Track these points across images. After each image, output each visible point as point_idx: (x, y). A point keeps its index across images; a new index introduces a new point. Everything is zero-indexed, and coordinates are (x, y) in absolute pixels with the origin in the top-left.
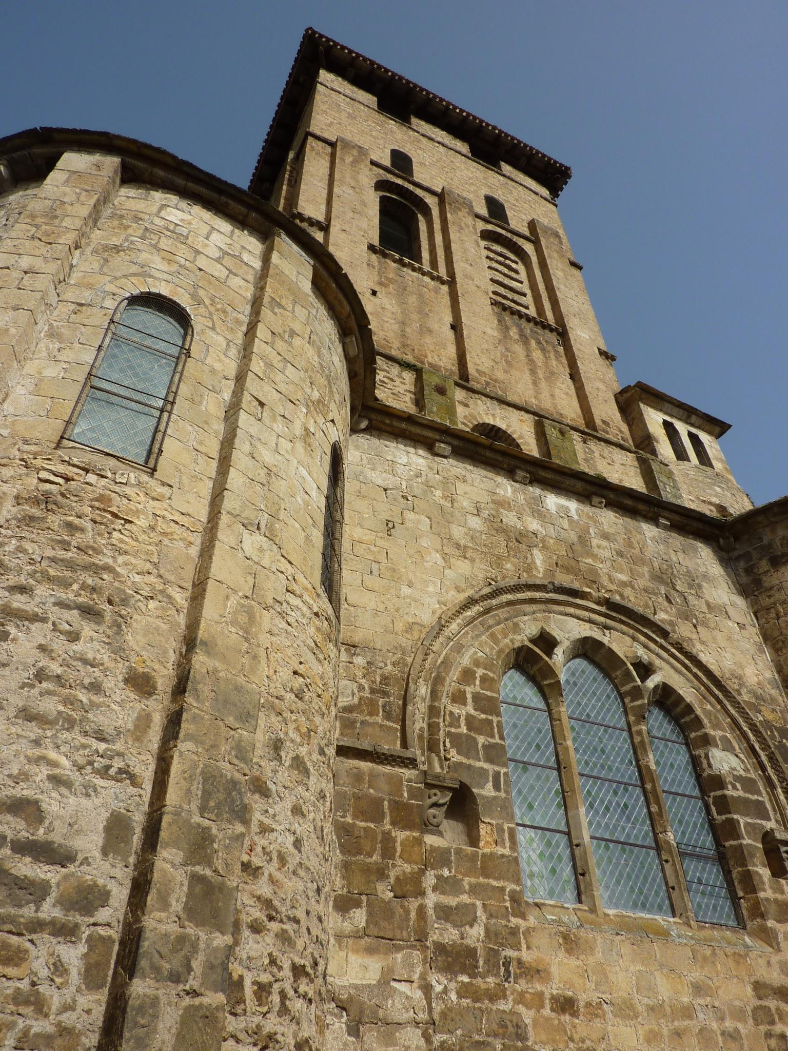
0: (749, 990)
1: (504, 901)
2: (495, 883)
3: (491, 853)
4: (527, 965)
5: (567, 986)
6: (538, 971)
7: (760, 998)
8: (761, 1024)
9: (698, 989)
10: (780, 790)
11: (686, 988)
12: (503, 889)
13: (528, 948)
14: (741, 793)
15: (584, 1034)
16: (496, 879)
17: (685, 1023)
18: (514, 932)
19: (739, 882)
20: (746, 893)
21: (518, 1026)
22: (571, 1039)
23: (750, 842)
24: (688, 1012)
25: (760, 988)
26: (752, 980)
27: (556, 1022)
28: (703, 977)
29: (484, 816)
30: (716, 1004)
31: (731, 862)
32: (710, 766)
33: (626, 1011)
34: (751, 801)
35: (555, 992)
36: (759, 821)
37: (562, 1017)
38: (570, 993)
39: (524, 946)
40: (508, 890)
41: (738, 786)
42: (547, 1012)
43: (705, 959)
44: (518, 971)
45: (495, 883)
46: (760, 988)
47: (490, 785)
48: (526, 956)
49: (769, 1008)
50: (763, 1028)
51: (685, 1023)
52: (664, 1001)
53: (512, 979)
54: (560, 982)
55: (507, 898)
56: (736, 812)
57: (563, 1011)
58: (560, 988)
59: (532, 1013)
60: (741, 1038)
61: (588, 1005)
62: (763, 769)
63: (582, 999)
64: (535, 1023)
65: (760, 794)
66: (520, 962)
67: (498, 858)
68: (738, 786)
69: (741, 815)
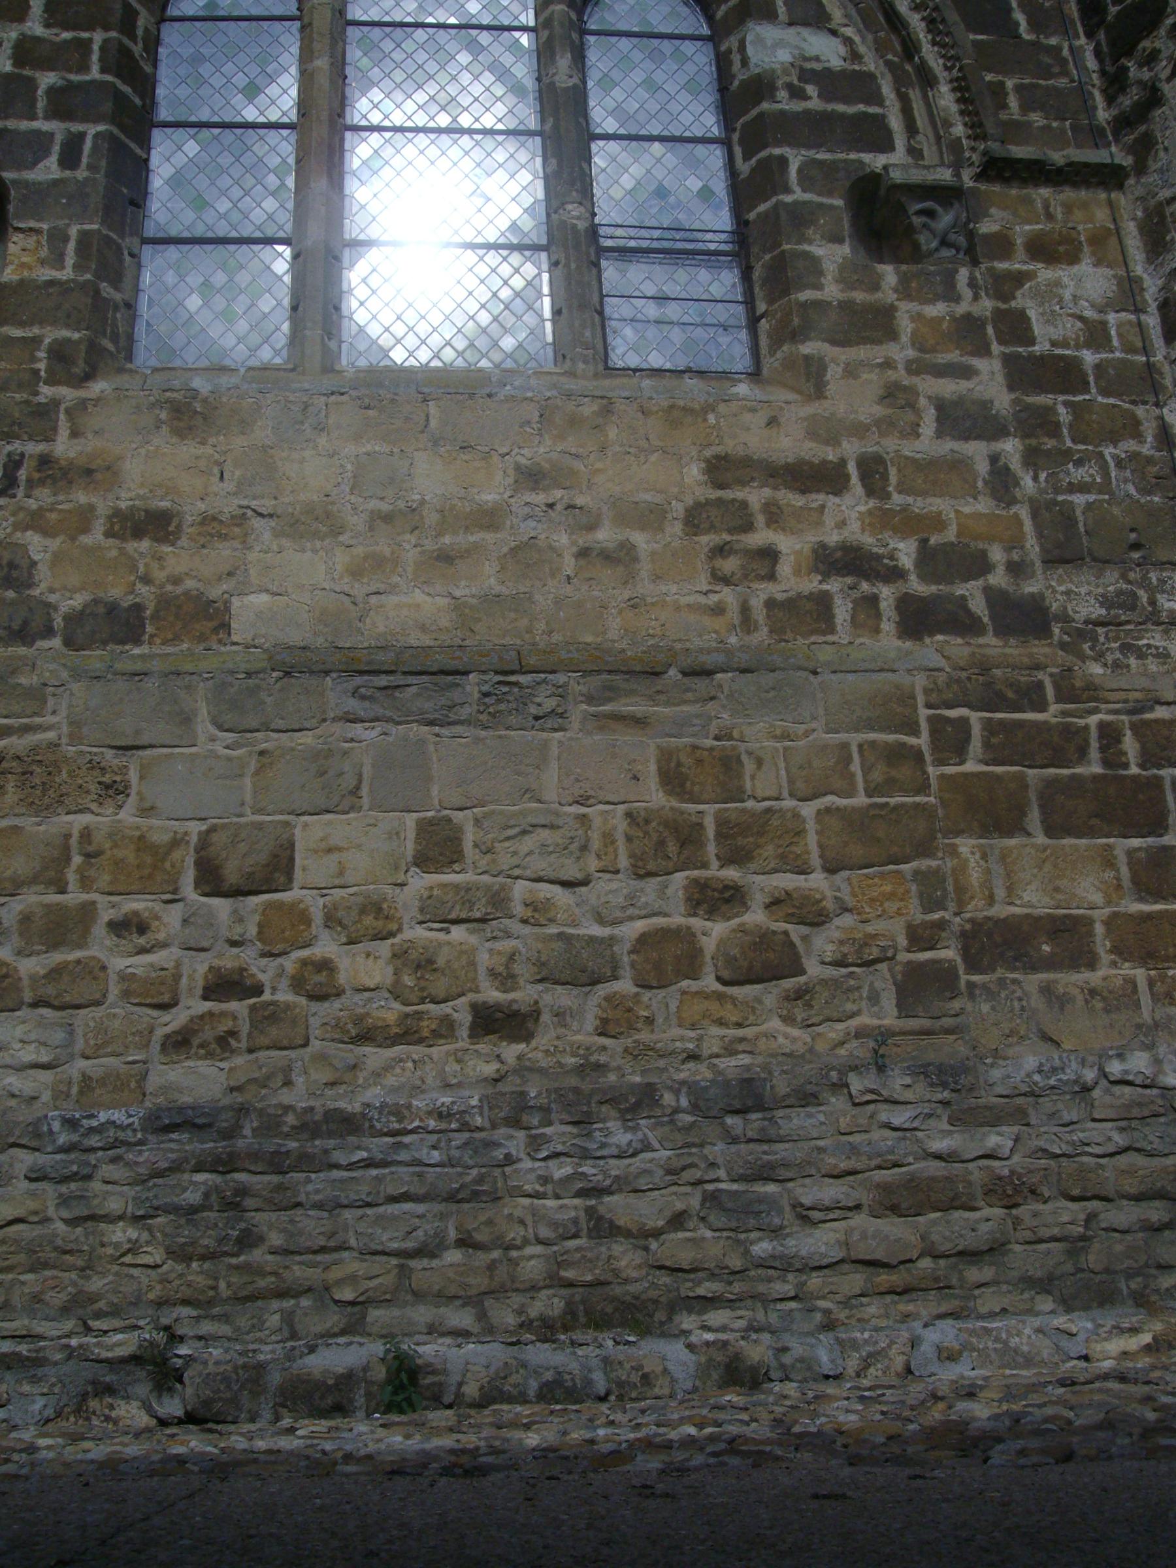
0: (694, 472)
1: (34, 359)
2: (17, 333)
3: (22, 281)
4: (63, 463)
5: (159, 492)
6: (89, 472)
7: (721, 486)
8: (707, 532)
9: (532, 477)
10: (944, 88)
11: (499, 476)
12: (36, 341)
13: (75, 434)
14: (815, 103)
15: (180, 569)
16: (22, 324)
17: (472, 539)
18: (45, 413)
19: (762, 286)
20: (771, 301)
21: (12, 565)
22: (146, 580)
23: (808, 196)
24: (489, 519)
25: (722, 469)
26: (708, 453)
27: (114, 553)
28: (554, 456)
29: (19, 217)
30: (580, 501)
31: (755, 249)
32: (745, 62)
33: (314, 524)
34: (842, 116)
35: (123, 505)
36: (853, 156)
37: (132, 546)
38: (165, 504)
39: (64, 432)
40: (47, 341)
41: (811, 90)
42: (96, 536)
43: (574, 421)
44: (36, 475)
45: (17, 333)
46: (722, 469)
47: (52, 161)
48: (63, 447)
49: (744, 505)
50: (707, 540)
51: (472, 539)
52: (423, 502)
53: (20, 493)
54: (142, 485)
55: (42, 354)
56: (779, 143)
57: (138, 534)
58: (139, 497)
59: (55, 544)
60: (636, 559)
61: (207, 520)
62: (910, 49)
63: (192, 510)
64: (57, 559)
65: (879, 100)
66: (45, 461)
67: (38, 287)
68: (811, 90)
69: (790, 145)
